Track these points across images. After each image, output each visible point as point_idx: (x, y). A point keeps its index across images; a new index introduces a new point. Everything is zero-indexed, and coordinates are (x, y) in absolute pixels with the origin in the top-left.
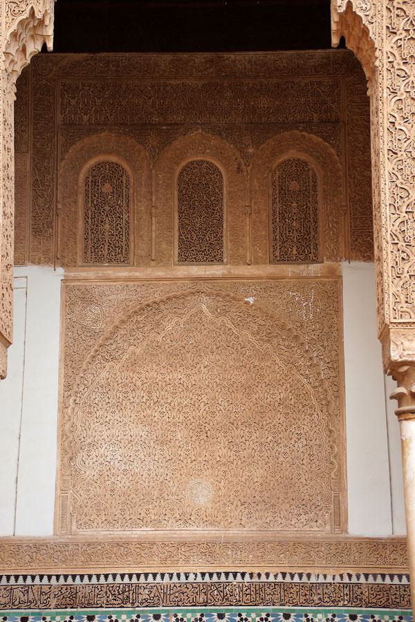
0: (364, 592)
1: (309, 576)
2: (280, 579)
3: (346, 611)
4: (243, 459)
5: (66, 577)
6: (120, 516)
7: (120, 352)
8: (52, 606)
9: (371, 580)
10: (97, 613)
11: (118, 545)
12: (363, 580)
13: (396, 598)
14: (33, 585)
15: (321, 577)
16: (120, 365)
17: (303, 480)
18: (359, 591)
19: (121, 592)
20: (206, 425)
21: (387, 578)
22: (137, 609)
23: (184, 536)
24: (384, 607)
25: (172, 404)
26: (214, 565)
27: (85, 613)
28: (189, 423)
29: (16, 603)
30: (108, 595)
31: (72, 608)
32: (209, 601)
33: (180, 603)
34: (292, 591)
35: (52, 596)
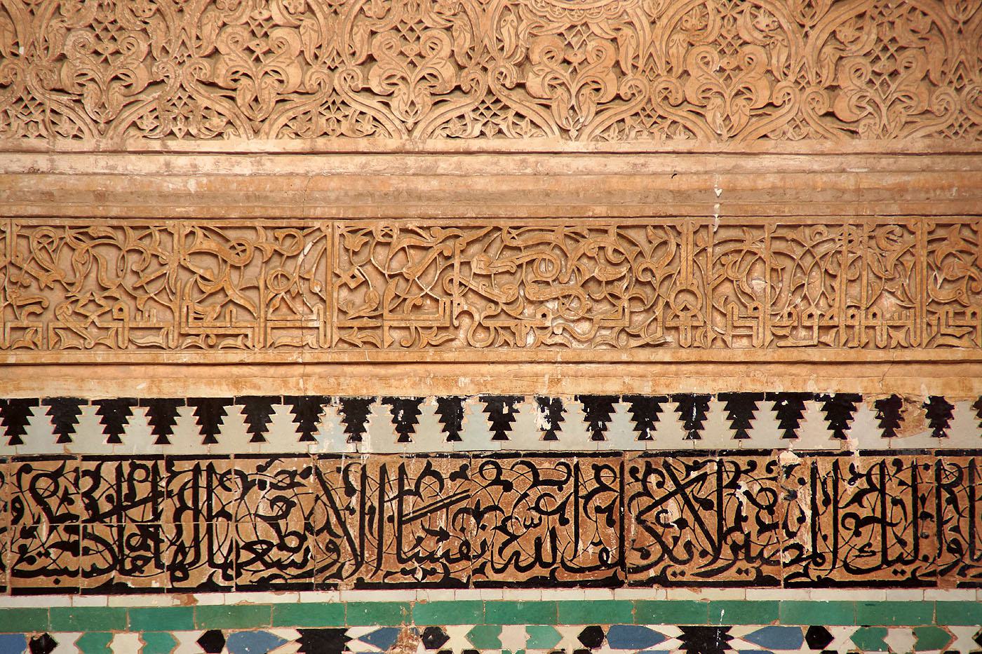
6: (91, 66)
11: (83, 233)
19: (105, 507)
22: (204, 599)
23: (480, 184)
26: (662, 355)
30: (27, 520)
32: (634, 559)
33: (461, 570)
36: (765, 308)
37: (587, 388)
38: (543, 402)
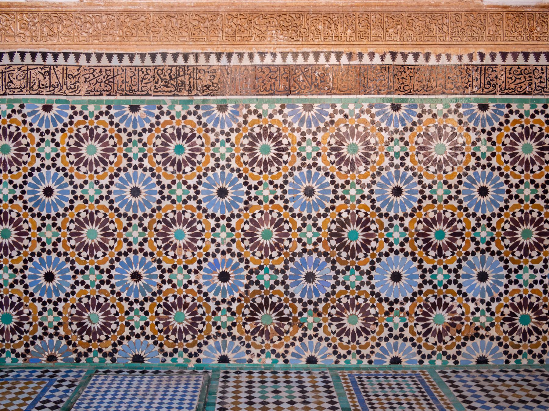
0: (499, 76)
1: (427, 56)
2: (388, 60)
3: (475, 100)
5: (99, 56)
8: (83, 92)
9: (510, 60)
10: (143, 102)
11: (168, 15)
12: (498, 60)
13: (541, 82)
14: (56, 66)
15: (444, 58)
18: (494, 74)
19: (173, 77)
21: (532, 57)
22: (195, 98)
24: (525, 94)
26: (299, 43)
27: (126, 102)
29: (35, 87)
30: (156, 80)
31: (109, 95)
32: (292, 89)
34: (404, 75)
35: (82, 79)
36: (322, 32)
37: (281, 50)
38: (272, 54)
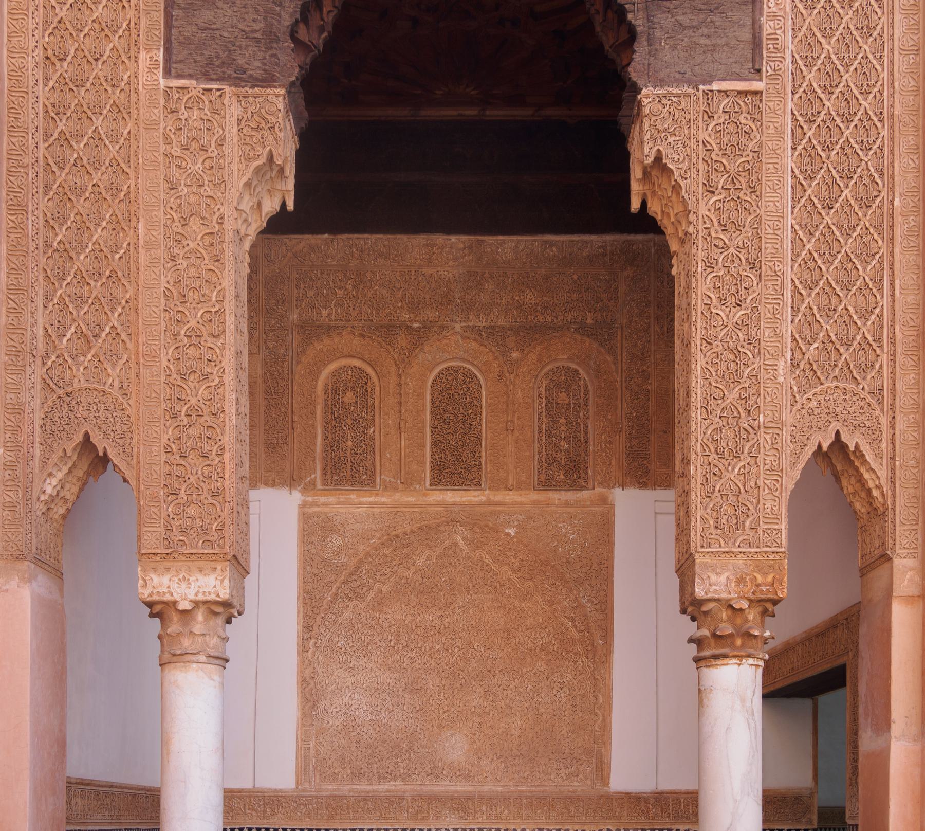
4: (500, 710)
7: (365, 589)
16: (365, 604)
17: (564, 732)
20: (461, 672)
25: (423, 649)
28: (441, 670)
